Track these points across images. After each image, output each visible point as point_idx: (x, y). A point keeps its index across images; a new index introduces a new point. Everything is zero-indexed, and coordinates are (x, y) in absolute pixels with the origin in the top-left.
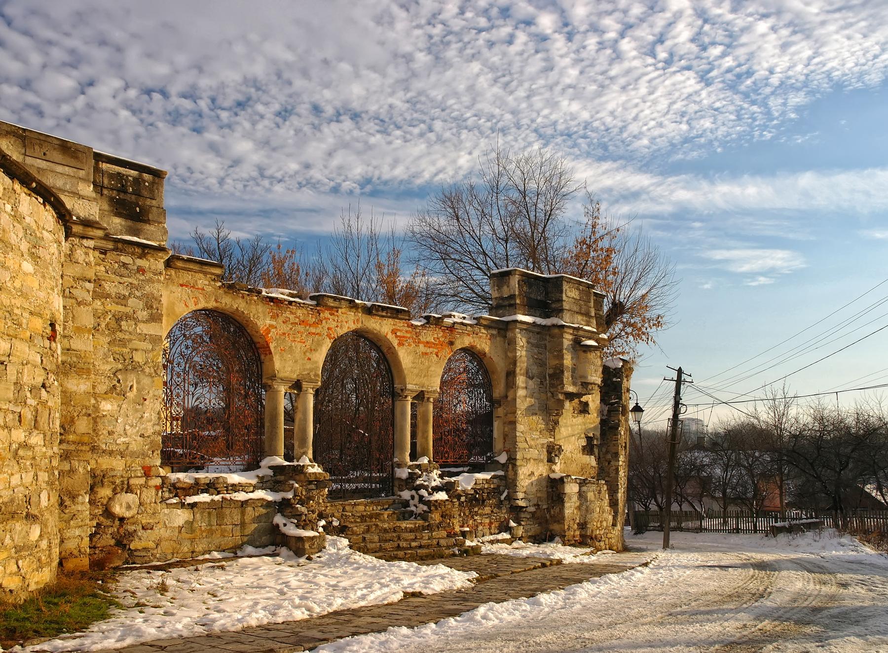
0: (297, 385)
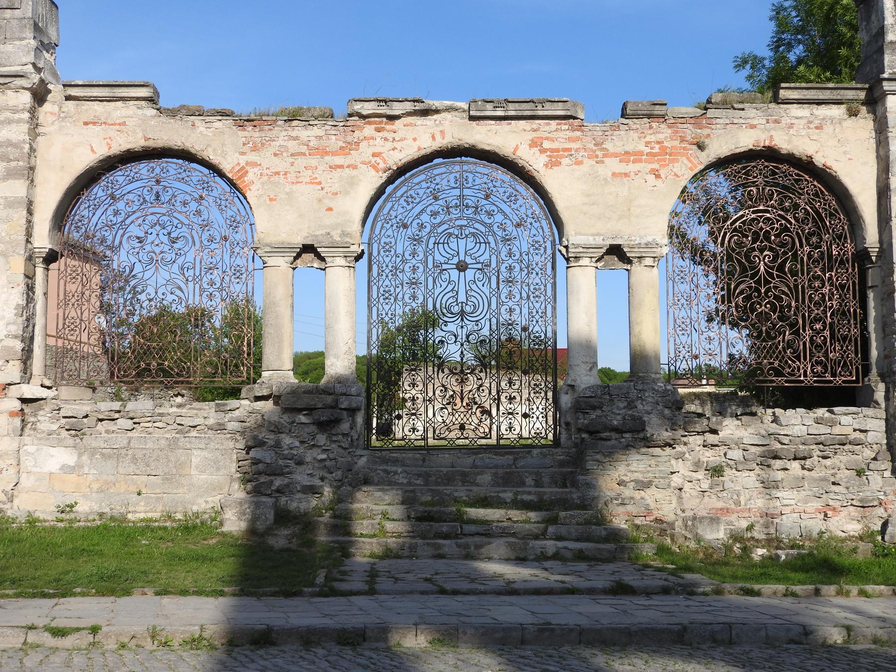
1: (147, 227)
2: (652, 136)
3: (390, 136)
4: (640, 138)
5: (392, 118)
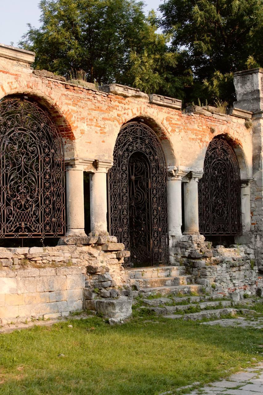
0: (95, 164)
5: (126, 97)
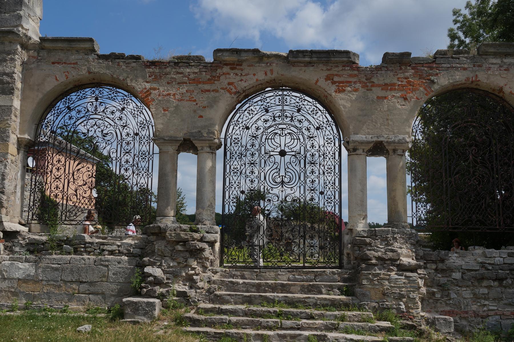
1: (88, 127)
2: (402, 74)
3: (239, 72)
4: (394, 75)
